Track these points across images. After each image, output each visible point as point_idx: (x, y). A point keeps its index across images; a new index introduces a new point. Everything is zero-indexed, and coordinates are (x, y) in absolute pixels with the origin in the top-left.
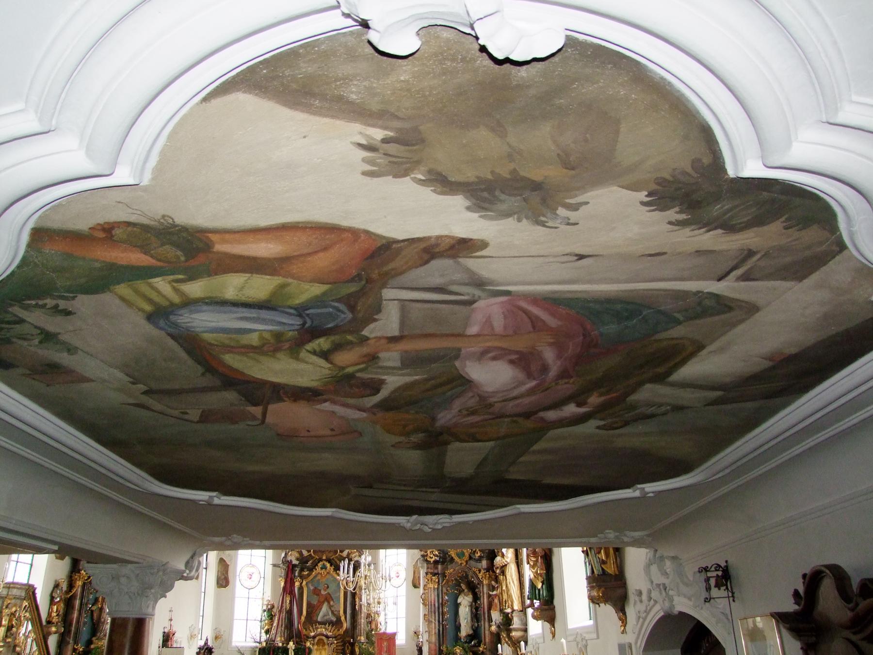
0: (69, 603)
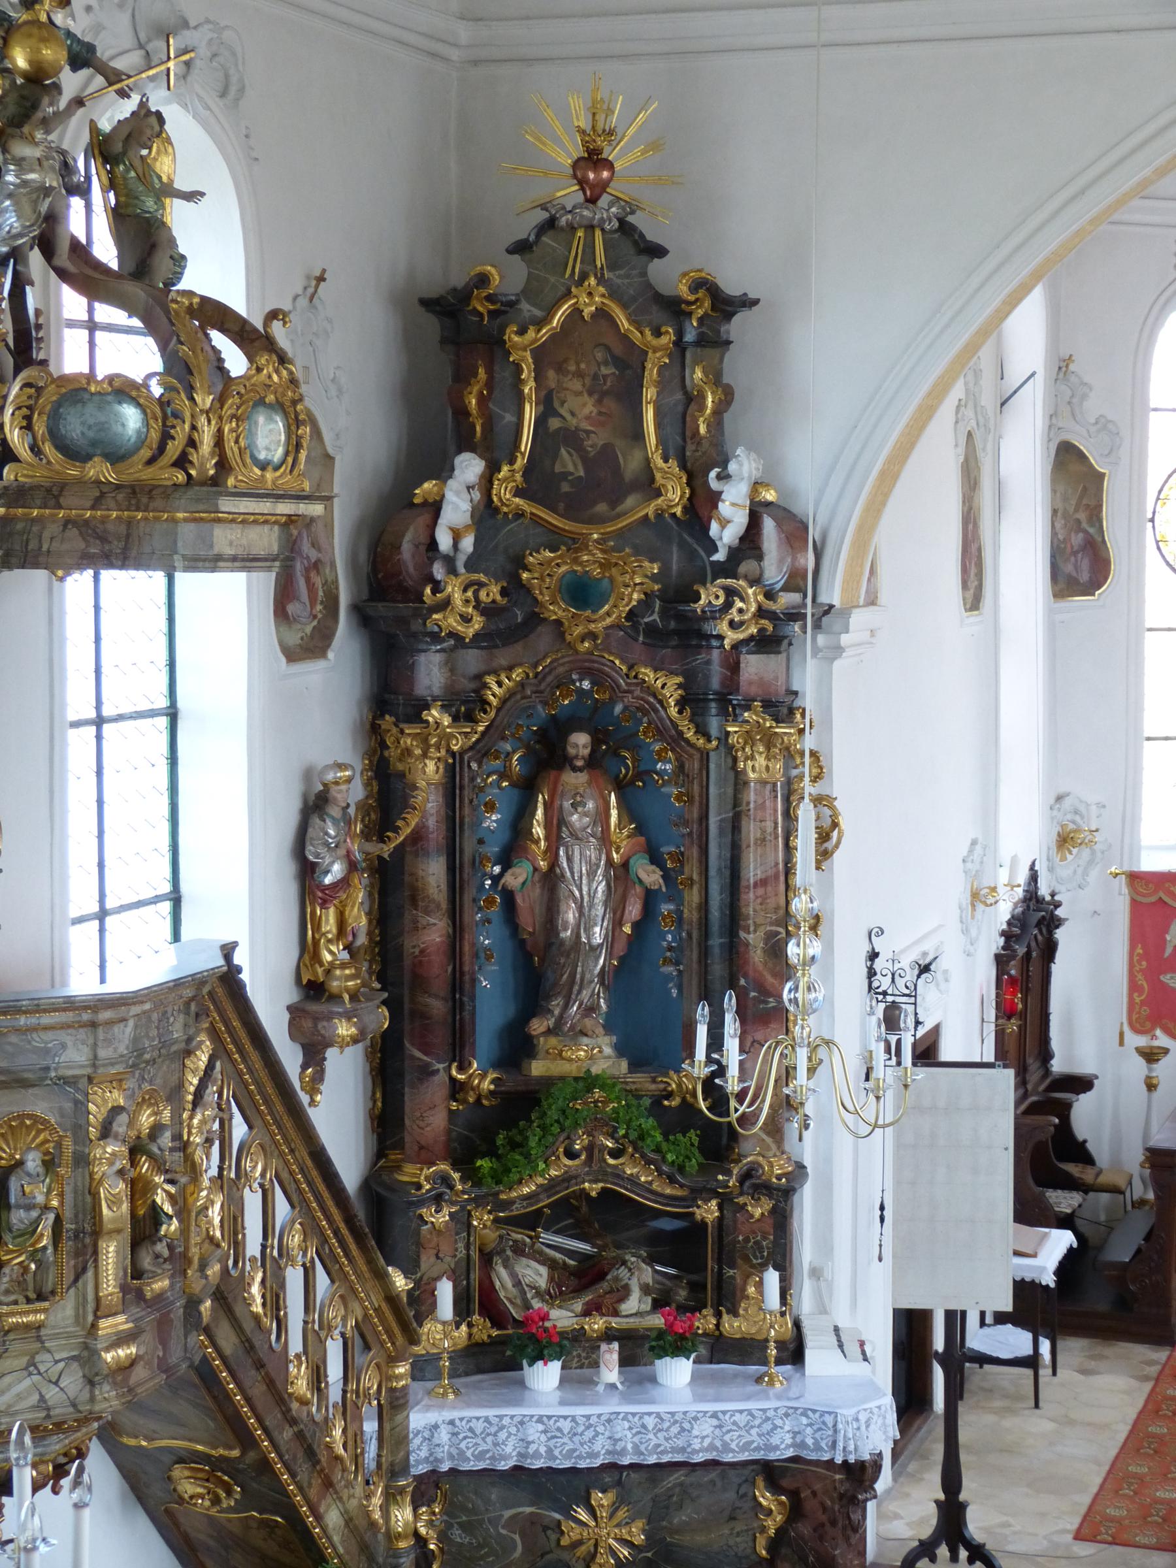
0: (390, 883)
